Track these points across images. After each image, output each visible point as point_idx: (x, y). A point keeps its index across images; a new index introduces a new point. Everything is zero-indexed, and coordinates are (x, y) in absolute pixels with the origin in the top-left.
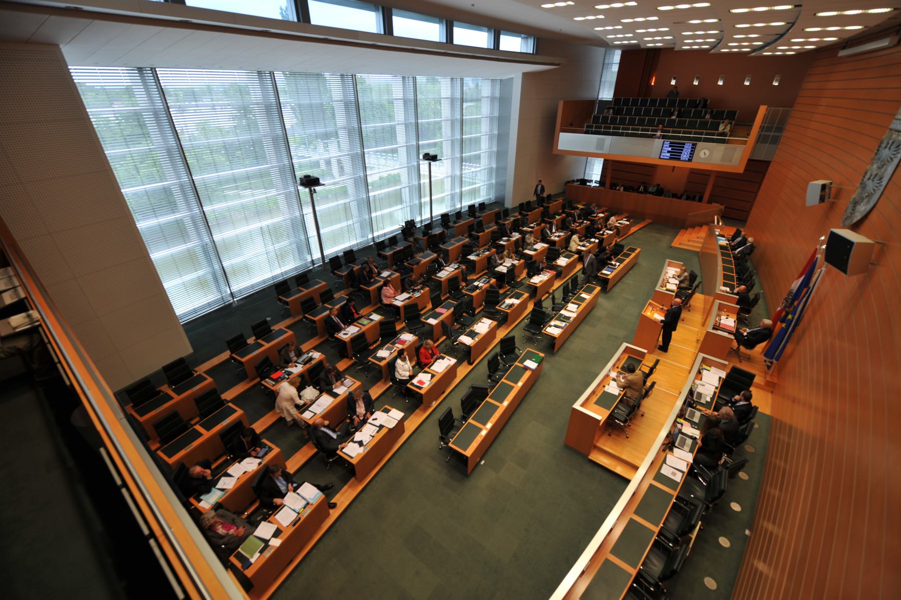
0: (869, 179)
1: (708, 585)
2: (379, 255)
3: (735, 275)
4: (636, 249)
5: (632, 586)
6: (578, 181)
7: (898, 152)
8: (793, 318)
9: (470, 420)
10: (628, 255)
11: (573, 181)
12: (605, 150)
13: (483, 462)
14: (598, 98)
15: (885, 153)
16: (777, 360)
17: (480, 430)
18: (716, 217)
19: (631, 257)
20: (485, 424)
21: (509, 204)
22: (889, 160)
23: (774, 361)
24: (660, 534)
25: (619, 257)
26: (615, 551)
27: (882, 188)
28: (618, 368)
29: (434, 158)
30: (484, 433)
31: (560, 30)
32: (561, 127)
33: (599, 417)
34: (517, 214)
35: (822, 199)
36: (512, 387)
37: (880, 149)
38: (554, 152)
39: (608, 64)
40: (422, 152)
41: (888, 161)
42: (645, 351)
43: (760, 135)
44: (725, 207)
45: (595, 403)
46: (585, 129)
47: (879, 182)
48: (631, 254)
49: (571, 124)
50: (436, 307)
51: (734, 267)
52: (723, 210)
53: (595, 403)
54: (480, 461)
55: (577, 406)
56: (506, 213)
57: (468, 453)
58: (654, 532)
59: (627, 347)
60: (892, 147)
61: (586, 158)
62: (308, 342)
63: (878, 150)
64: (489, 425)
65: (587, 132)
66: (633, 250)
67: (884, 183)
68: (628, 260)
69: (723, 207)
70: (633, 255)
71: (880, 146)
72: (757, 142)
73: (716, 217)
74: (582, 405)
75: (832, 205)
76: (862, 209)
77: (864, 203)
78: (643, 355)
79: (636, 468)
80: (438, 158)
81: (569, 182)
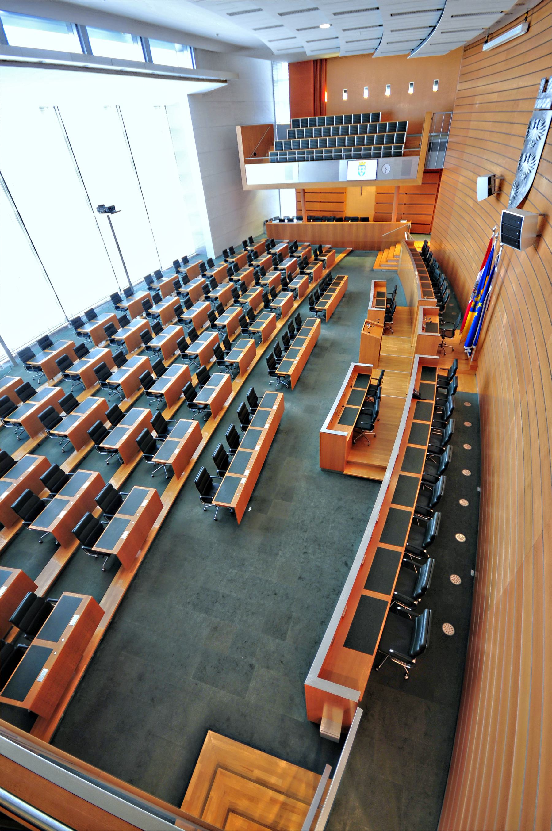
0: (525, 161)
1: (459, 540)
2: (79, 334)
3: (430, 282)
4: (344, 277)
5: (403, 560)
6: (276, 219)
7: (544, 129)
8: (482, 305)
9: (227, 474)
10: (337, 284)
11: (271, 220)
12: (295, 180)
13: (250, 509)
14: (275, 122)
15: (534, 133)
16: (475, 345)
17: (240, 479)
18: (406, 233)
19: (341, 285)
20: (242, 473)
21: (211, 254)
22: (538, 139)
23: (474, 347)
24: (416, 512)
25: (330, 287)
26: (394, 502)
27: (536, 167)
28: (351, 387)
29: (112, 210)
30: (243, 481)
31: (218, 35)
32: (245, 158)
33: (345, 434)
34: (223, 263)
35: (490, 193)
36: (261, 431)
37: (530, 131)
38: (245, 188)
39: (278, 81)
40: (95, 206)
41: (537, 140)
42: (372, 366)
43: (430, 143)
44: (412, 224)
45: (339, 423)
46: (270, 157)
47: (533, 161)
48: (340, 282)
49: (255, 155)
50: (160, 376)
51: (428, 275)
52: (411, 227)
53: (339, 423)
54: (248, 508)
55: (324, 429)
56: (211, 263)
57: (233, 504)
58: (411, 513)
59: (355, 366)
60: (539, 126)
61: (277, 190)
62: (20, 449)
63: (528, 132)
64: (247, 473)
65: (273, 162)
66: (341, 278)
67: (537, 162)
68: (339, 288)
69: (410, 223)
70: (343, 282)
71: (529, 128)
72: (429, 151)
73: (406, 233)
74: (329, 427)
75: (499, 196)
76: (524, 190)
77: (524, 184)
78: (370, 369)
79: (384, 469)
80: (117, 210)
81: (267, 221)
